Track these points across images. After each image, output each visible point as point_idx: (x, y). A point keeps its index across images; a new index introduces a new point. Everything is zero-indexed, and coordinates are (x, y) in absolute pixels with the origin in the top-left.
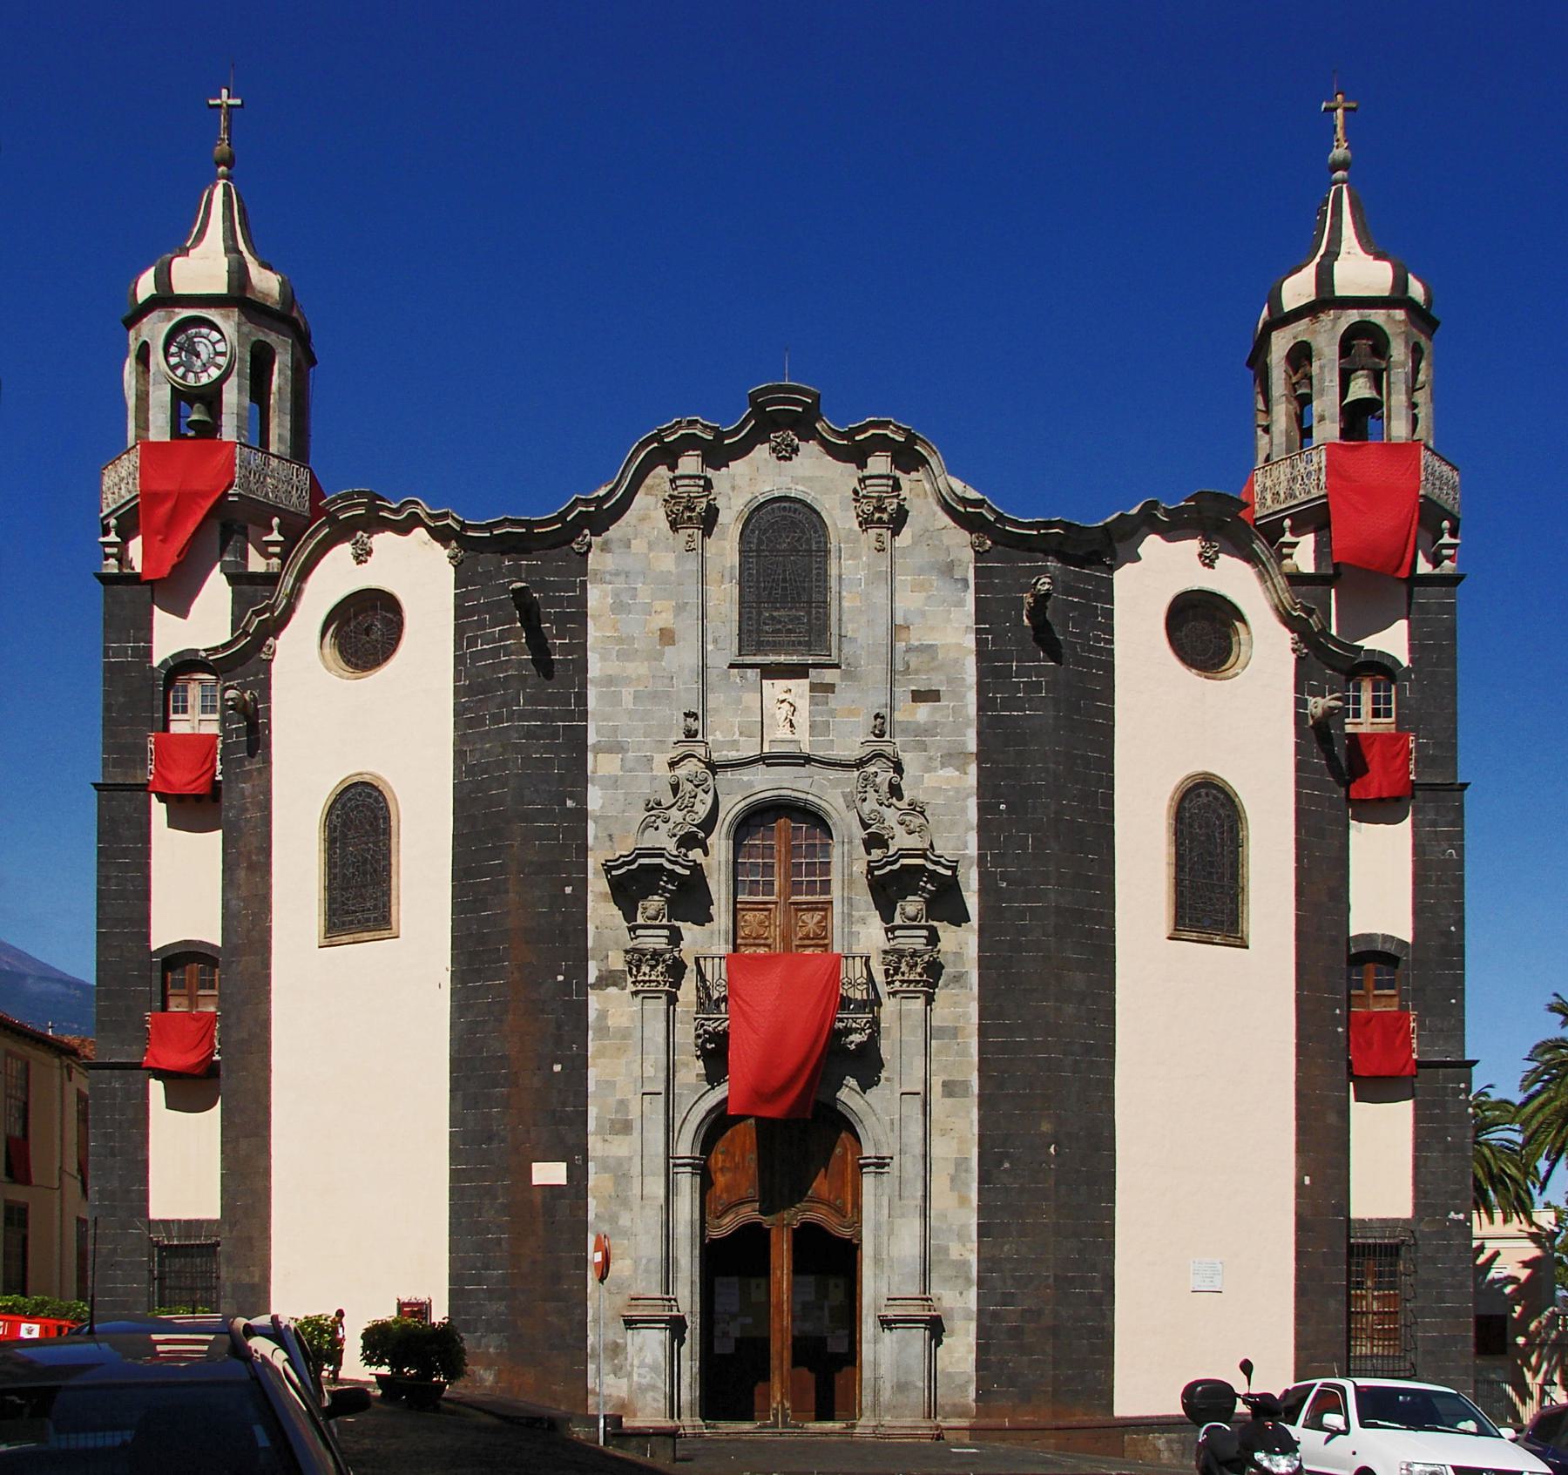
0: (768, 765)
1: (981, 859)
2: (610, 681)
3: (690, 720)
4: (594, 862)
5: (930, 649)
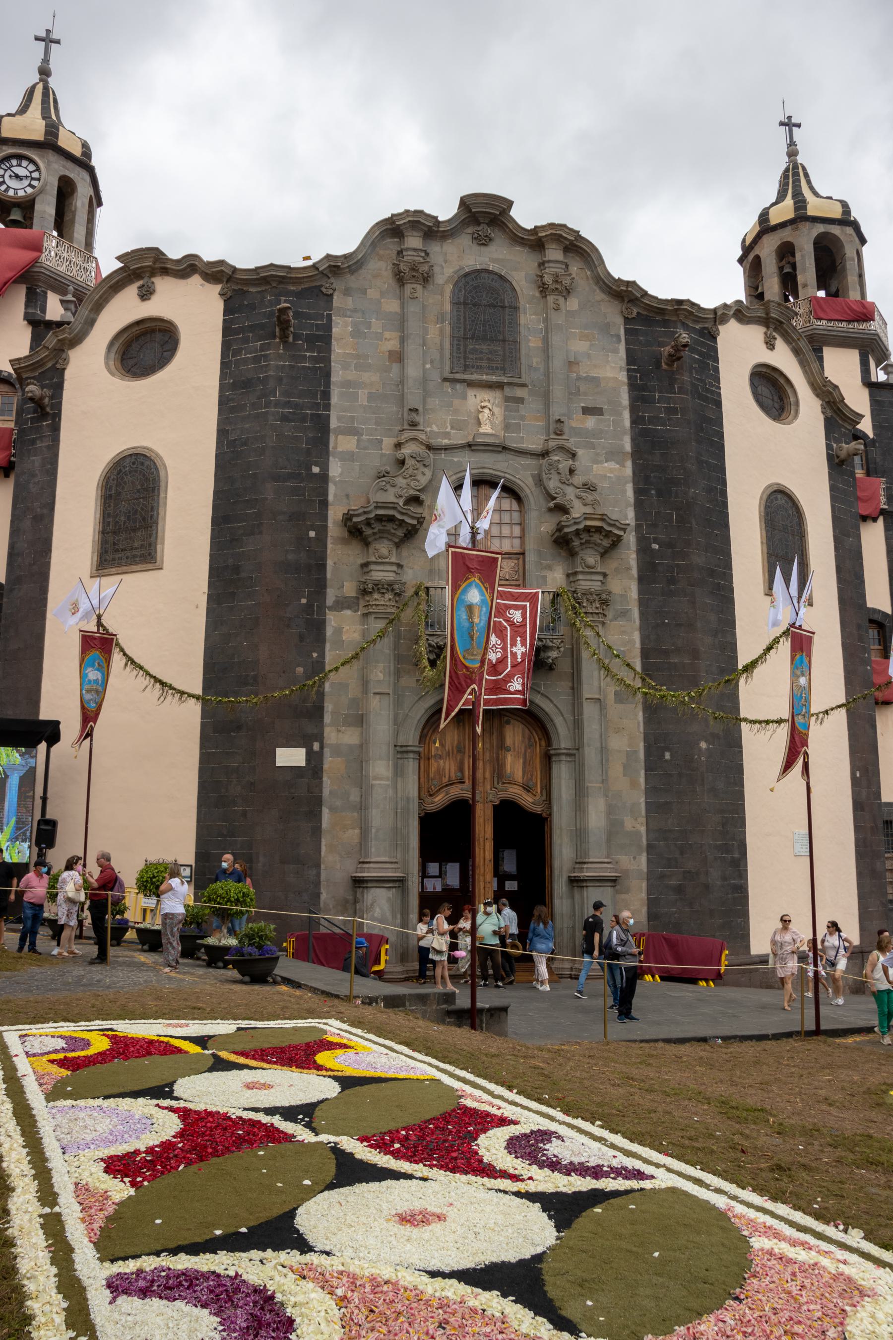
0: (473, 450)
1: (638, 527)
2: (347, 384)
3: (414, 415)
4: (335, 513)
5: (595, 381)
